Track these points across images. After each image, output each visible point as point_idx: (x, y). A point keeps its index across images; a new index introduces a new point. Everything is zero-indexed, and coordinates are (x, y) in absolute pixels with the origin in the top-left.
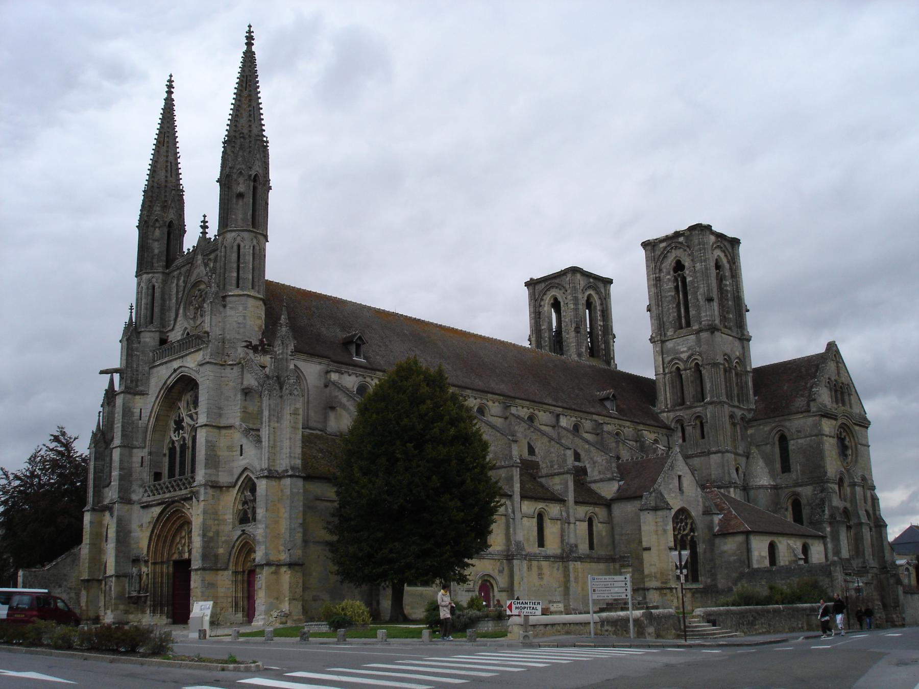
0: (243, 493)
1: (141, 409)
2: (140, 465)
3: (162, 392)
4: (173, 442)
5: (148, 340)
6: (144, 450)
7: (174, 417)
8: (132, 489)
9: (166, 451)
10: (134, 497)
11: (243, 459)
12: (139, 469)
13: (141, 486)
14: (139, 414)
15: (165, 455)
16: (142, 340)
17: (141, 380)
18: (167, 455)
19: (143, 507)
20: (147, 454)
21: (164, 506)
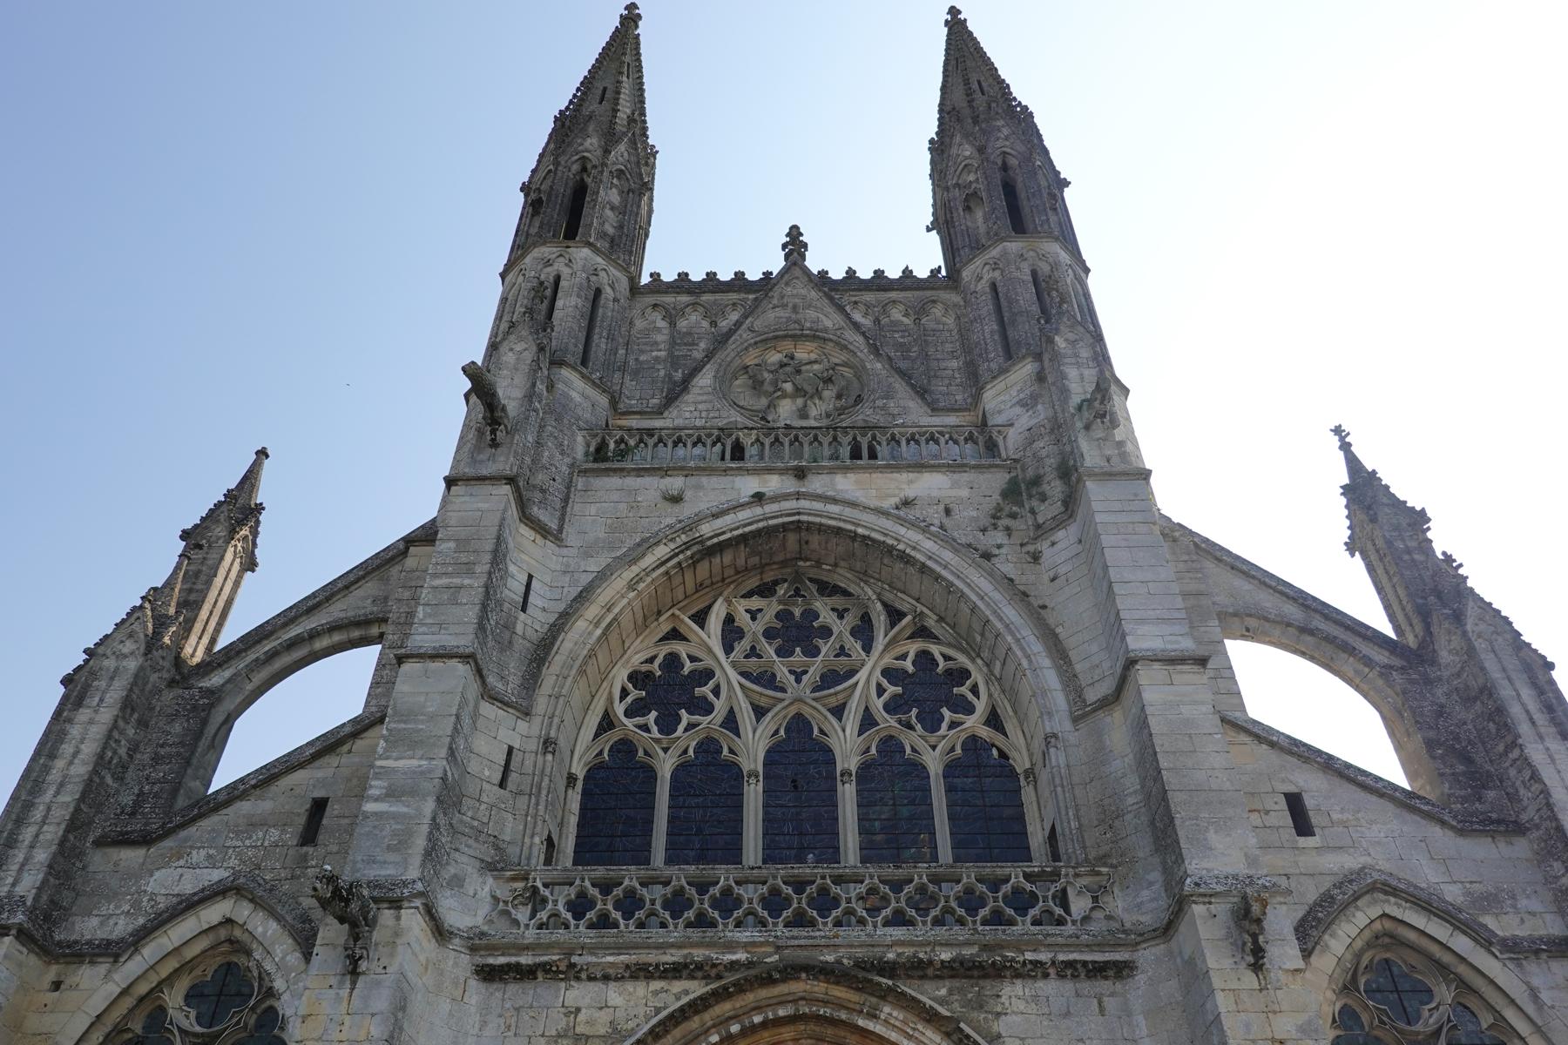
0: (1345, 987)
1: (530, 577)
2: (497, 777)
3: (662, 551)
4: (625, 747)
5: (574, 394)
6: (522, 726)
7: (641, 652)
8: (452, 870)
9: (579, 770)
10: (457, 915)
11: (1319, 850)
12: (492, 793)
13: (491, 867)
14: (523, 589)
15: (571, 779)
16: (560, 386)
17: (543, 491)
18: (580, 784)
19: (489, 974)
20: (533, 745)
21: (697, 988)
